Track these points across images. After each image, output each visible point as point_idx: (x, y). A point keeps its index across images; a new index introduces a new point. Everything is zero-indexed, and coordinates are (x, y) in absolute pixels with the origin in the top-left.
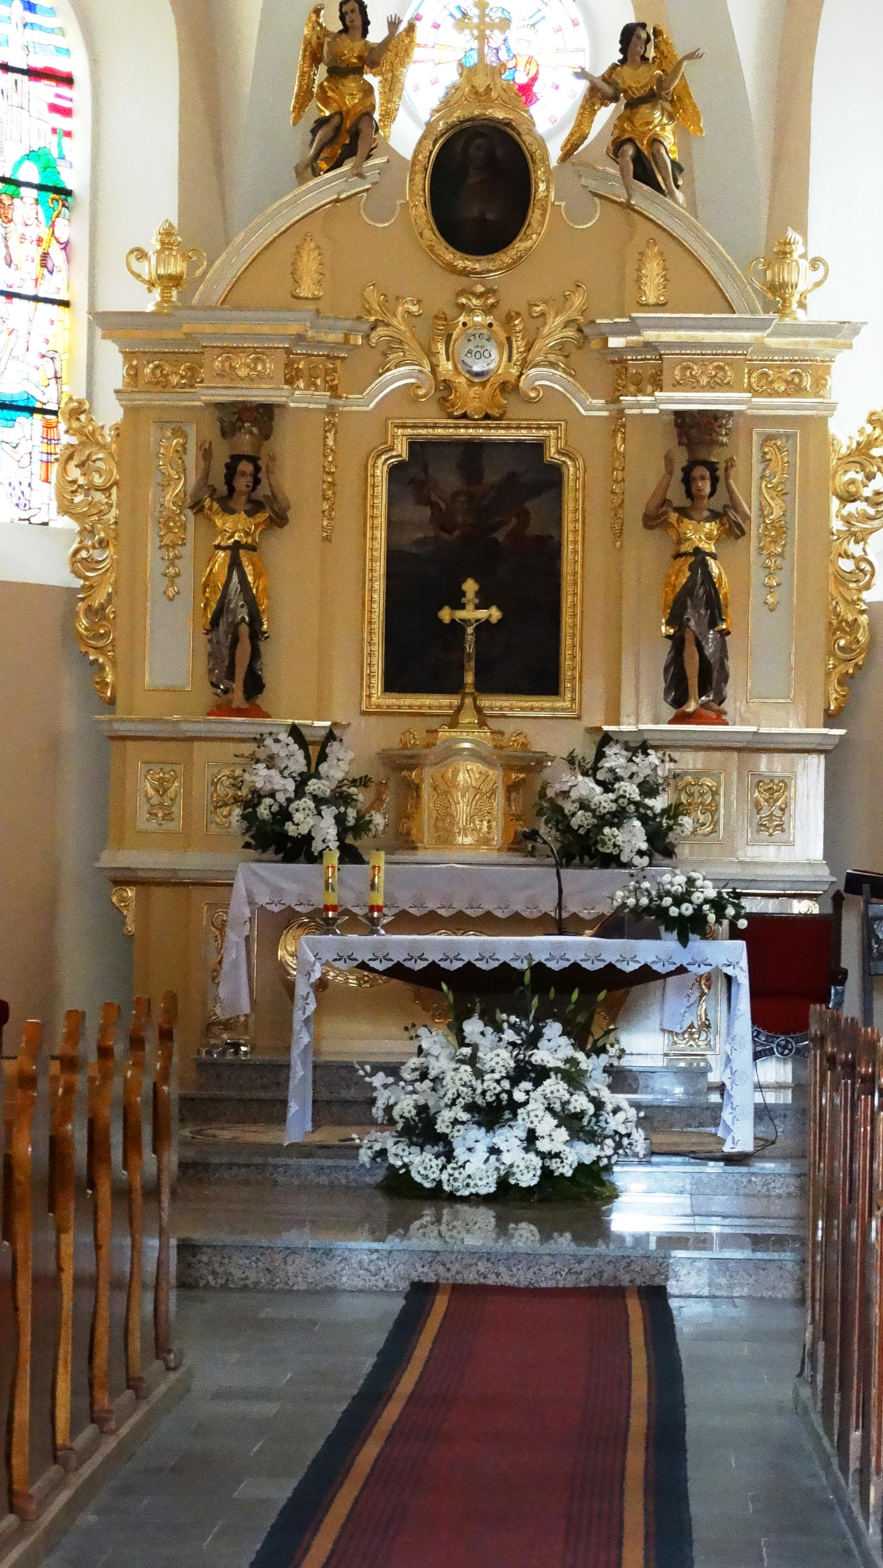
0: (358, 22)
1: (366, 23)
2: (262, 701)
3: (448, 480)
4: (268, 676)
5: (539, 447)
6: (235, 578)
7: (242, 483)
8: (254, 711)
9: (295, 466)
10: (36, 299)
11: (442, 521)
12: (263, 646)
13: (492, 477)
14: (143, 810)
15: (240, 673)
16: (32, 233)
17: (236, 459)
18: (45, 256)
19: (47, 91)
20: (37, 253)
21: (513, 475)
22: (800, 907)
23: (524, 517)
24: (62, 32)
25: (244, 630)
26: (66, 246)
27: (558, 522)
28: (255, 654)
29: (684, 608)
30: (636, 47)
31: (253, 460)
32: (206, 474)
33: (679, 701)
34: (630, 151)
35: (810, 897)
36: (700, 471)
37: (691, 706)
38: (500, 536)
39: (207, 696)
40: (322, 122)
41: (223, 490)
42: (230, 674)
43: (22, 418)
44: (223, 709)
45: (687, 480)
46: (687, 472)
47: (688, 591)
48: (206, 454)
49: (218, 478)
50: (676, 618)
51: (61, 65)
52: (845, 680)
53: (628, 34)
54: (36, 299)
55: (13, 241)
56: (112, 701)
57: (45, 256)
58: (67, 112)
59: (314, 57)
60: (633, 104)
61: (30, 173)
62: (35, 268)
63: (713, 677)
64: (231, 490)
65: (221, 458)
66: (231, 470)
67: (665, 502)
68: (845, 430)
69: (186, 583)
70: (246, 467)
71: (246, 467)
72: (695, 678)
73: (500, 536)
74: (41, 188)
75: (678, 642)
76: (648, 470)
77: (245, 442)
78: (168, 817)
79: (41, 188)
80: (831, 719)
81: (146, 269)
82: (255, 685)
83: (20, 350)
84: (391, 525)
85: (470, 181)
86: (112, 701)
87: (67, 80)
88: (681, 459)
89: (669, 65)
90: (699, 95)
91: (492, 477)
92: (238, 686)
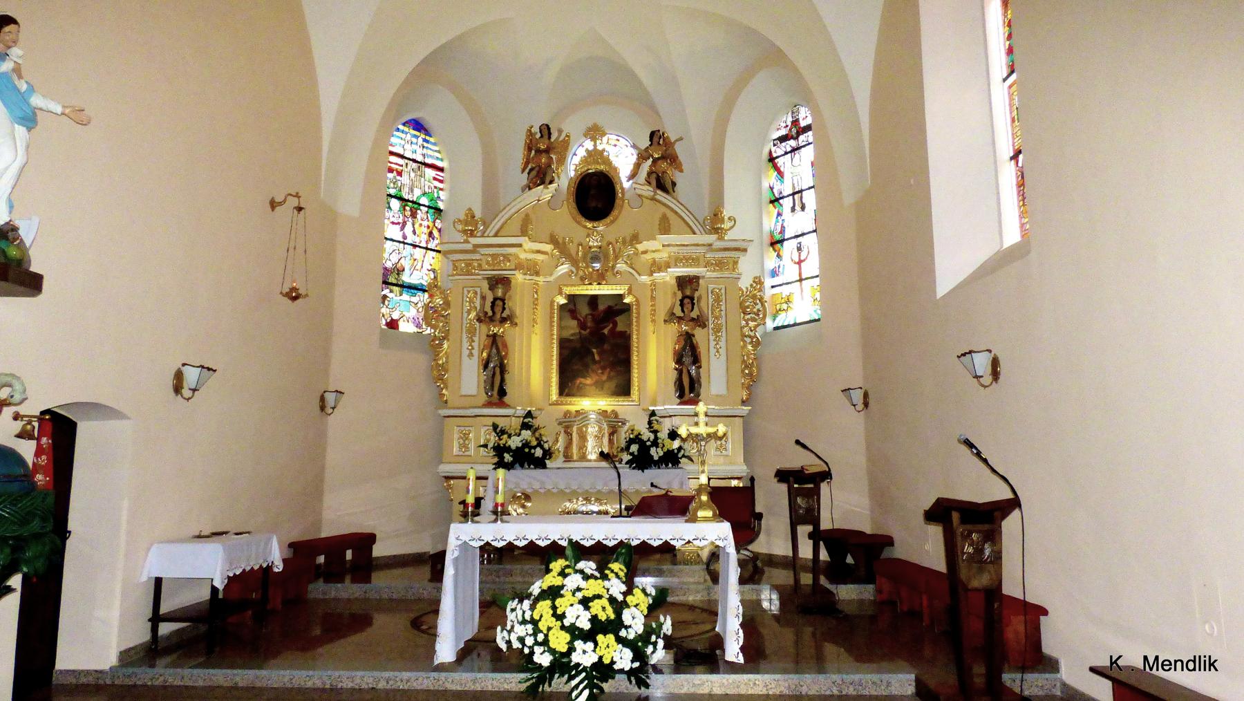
0: (546, 132)
1: (550, 134)
2: (506, 399)
3: (584, 310)
4: (508, 388)
5: (621, 297)
6: (494, 351)
7: (498, 309)
8: (501, 404)
9: (518, 302)
10: (427, 249)
11: (582, 326)
12: (507, 376)
13: (602, 307)
14: (456, 445)
15: (496, 389)
16: (425, 223)
17: (495, 299)
18: (431, 234)
19: (430, 173)
20: (427, 231)
21: (610, 307)
22: (734, 483)
23: (615, 324)
24: (439, 152)
25: (498, 370)
26: (440, 230)
27: (630, 325)
28: (503, 380)
29: (682, 356)
30: (655, 139)
31: (503, 300)
32: (483, 305)
33: (681, 396)
34: (654, 176)
35: (738, 478)
36: (686, 301)
37: (686, 398)
38: (606, 331)
39: (483, 398)
40: (531, 170)
41: (490, 313)
42: (492, 389)
43: (420, 293)
44: (489, 404)
45: (682, 305)
46: (682, 301)
47: (684, 349)
48: (483, 298)
49: (488, 308)
50: (679, 361)
51: (439, 164)
52: (749, 388)
53: (652, 135)
54: (427, 249)
55: (417, 226)
56: (446, 402)
57: (431, 234)
58: (441, 181)
59: (530, 149)
60: (655, 161)
61: (424, 201)
62: (425, 237)
63: (694, 384)
64: (494, 313)
65: (490, 298)
66: (493, 304)
67: (673, 314)
68: (745, 283)
69: (476, 352)
70: (499, 303)
71: (499, 303)
72: (688, 388)
73: (606, 331)
74: (429, 207)
75: (680, 372)
76: (668, 299)
77: (500, 293)
78: (467, 448)
79: (429, 207)
80: (744, 403)
81: (460, 227)
82: (502, 392)
83: (418, 267)
84: (560, 328)
85: (592, 192)
86: (446, 402)
87: (441, 170)
88: (680, 295)
89: (668, 144)
90: (682, 157)
91: (602, 307)
92: (495, 392)
